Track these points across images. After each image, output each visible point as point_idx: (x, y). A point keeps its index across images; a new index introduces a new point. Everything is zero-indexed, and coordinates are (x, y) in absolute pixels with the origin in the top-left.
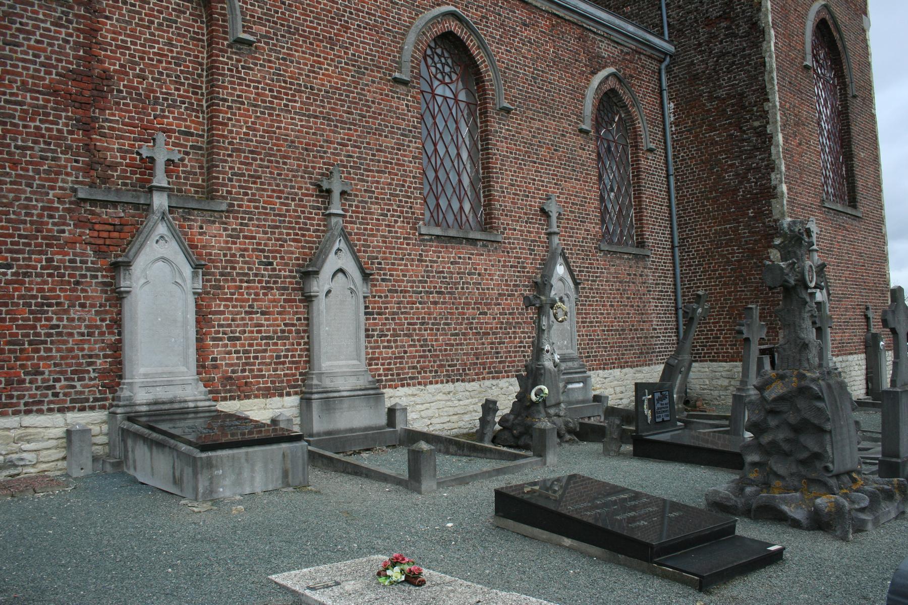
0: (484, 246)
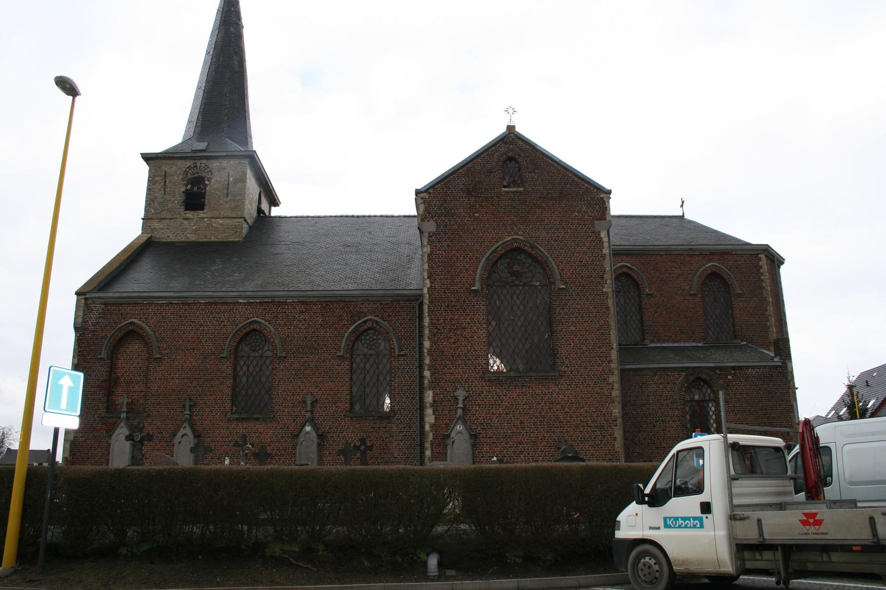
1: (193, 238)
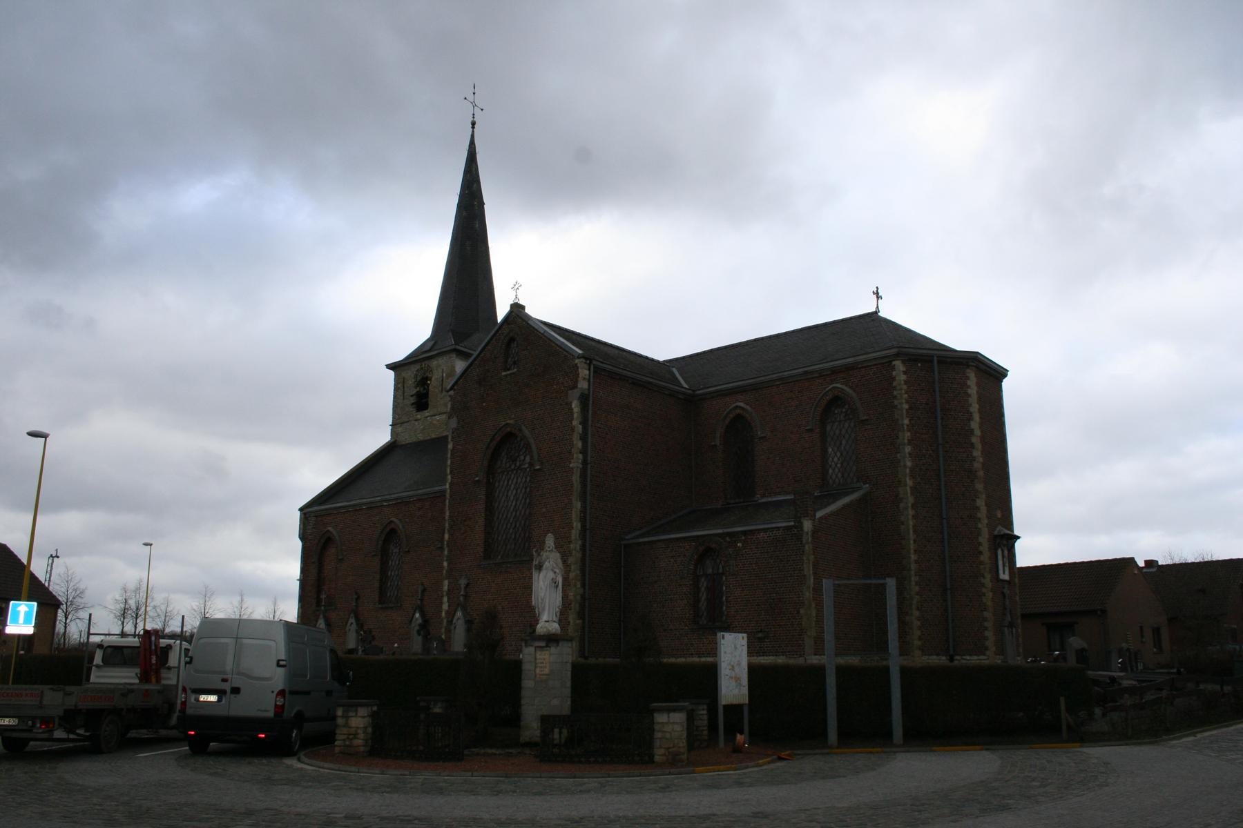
1: (421, 437)
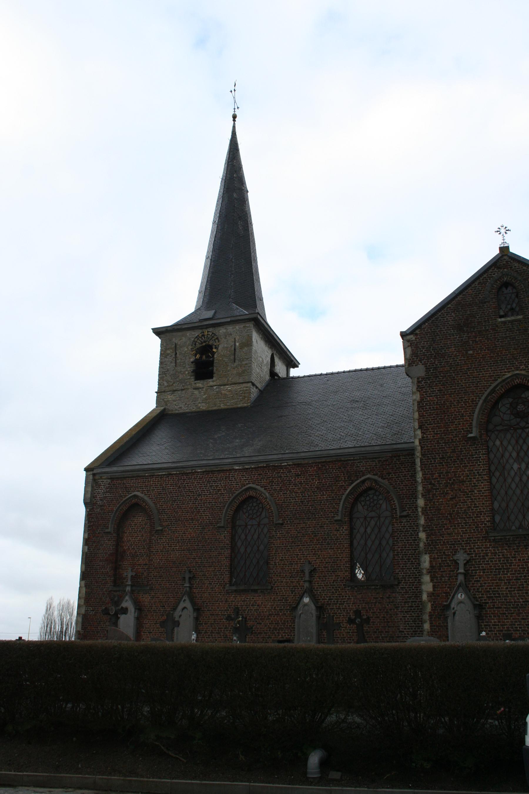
0: (261, 592)
1: (203, 407)
